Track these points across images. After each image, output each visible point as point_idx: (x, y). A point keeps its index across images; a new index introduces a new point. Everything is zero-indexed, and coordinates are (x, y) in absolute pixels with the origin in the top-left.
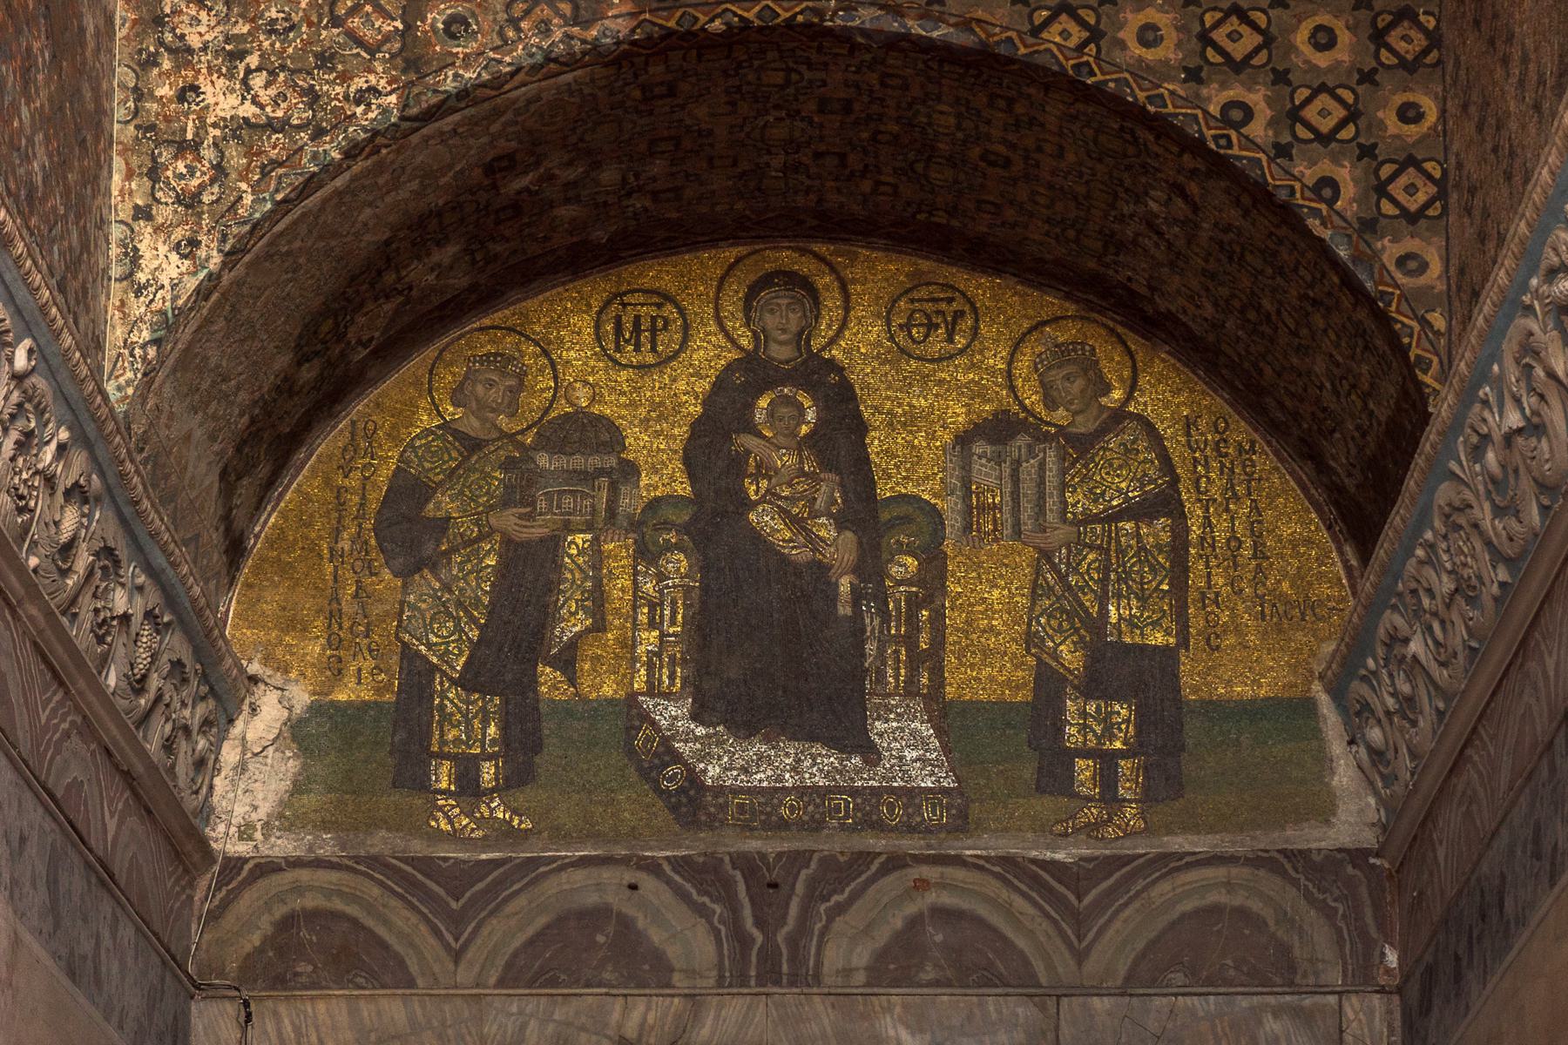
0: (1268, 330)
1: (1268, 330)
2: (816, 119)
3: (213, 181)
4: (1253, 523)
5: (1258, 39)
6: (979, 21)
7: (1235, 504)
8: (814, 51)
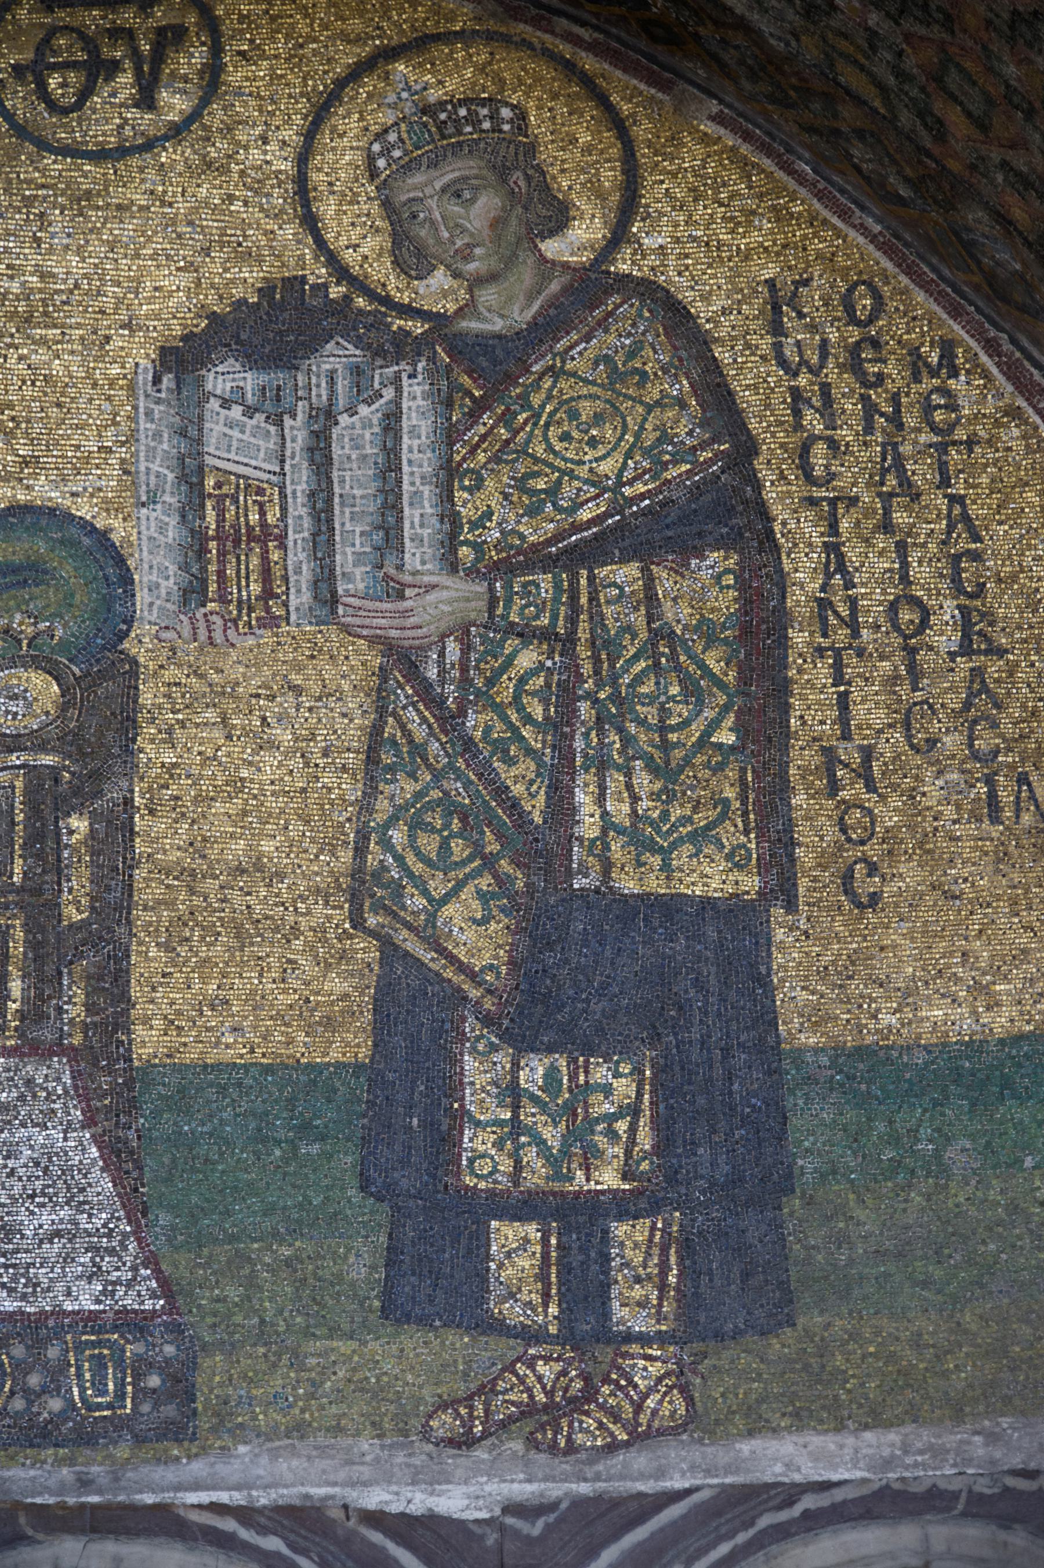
4: (957, 558)
7: (907, 508)
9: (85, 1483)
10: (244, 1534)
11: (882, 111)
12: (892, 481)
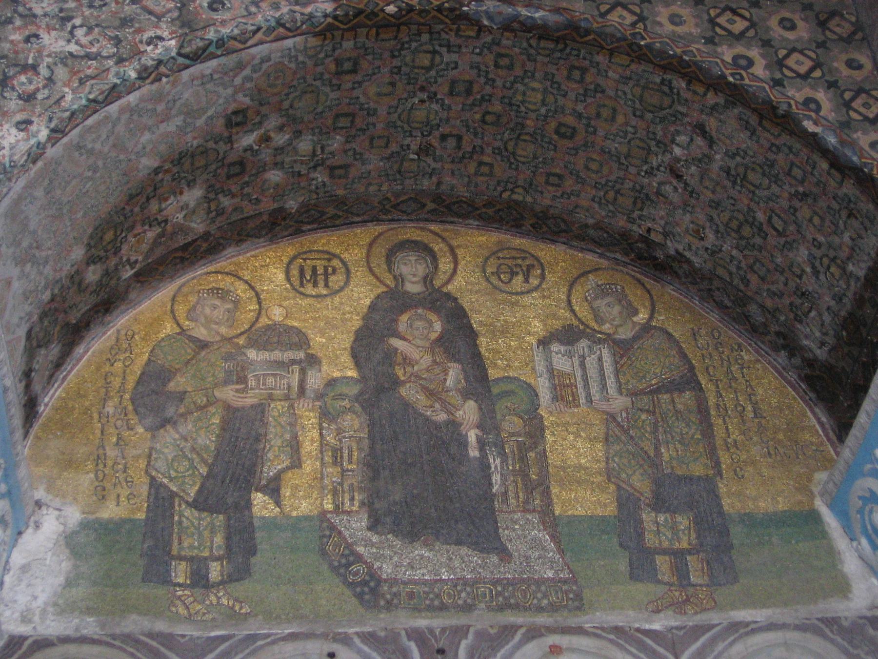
0: (758, 240)
1: (758, 240)
2: (446, 102)
3: (44, 87)
4: (750, 395)
5: (746, 24)
6: (564, 9)
8: (453, 34)
9: (556, 622)
10: (604, 634)
11: (728, 279)
12: (730, 376)
